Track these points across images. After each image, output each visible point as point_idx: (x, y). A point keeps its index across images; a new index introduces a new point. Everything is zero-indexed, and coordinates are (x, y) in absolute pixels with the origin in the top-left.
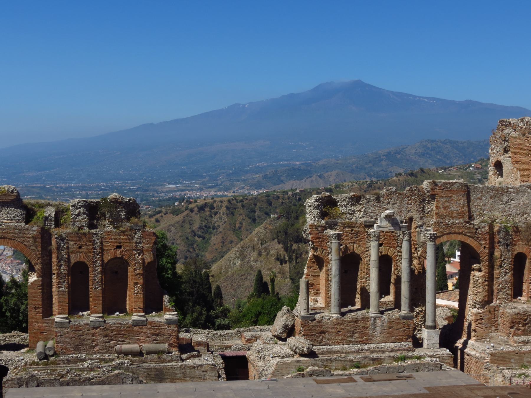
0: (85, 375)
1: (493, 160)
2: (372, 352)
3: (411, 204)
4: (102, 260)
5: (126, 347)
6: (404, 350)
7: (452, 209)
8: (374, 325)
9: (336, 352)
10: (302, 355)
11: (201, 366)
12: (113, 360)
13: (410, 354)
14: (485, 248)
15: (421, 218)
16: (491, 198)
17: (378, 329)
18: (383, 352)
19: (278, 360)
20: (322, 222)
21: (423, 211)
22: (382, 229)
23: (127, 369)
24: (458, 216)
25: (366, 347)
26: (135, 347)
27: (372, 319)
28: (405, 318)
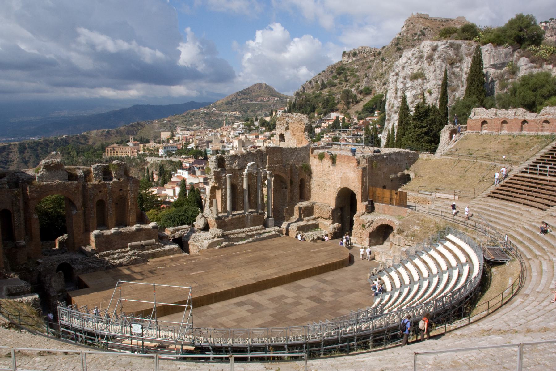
2: (248, 232)
5: (133, 243)
7: (275, 159)
10: (218, 237)
13: (265, 231)
15: (262, 165)
18: (253, 231)
20: (219, 170)
23: (138, 255)
24: (277, 163)
25: (244, 230)
26: (138, 243)
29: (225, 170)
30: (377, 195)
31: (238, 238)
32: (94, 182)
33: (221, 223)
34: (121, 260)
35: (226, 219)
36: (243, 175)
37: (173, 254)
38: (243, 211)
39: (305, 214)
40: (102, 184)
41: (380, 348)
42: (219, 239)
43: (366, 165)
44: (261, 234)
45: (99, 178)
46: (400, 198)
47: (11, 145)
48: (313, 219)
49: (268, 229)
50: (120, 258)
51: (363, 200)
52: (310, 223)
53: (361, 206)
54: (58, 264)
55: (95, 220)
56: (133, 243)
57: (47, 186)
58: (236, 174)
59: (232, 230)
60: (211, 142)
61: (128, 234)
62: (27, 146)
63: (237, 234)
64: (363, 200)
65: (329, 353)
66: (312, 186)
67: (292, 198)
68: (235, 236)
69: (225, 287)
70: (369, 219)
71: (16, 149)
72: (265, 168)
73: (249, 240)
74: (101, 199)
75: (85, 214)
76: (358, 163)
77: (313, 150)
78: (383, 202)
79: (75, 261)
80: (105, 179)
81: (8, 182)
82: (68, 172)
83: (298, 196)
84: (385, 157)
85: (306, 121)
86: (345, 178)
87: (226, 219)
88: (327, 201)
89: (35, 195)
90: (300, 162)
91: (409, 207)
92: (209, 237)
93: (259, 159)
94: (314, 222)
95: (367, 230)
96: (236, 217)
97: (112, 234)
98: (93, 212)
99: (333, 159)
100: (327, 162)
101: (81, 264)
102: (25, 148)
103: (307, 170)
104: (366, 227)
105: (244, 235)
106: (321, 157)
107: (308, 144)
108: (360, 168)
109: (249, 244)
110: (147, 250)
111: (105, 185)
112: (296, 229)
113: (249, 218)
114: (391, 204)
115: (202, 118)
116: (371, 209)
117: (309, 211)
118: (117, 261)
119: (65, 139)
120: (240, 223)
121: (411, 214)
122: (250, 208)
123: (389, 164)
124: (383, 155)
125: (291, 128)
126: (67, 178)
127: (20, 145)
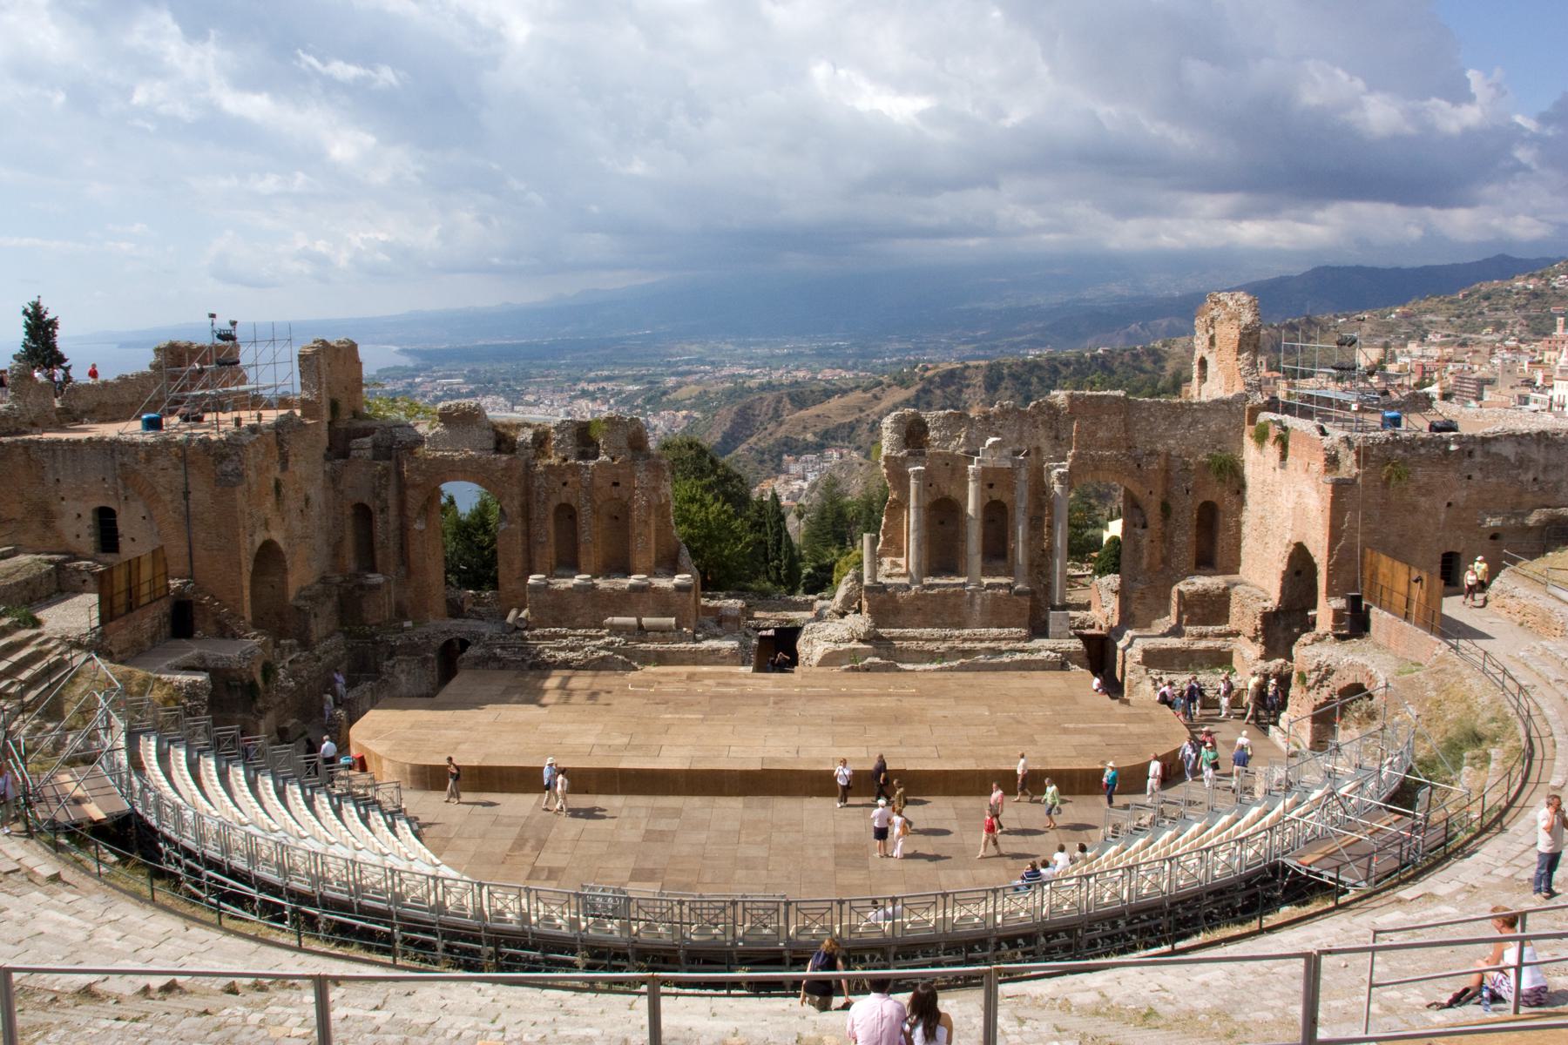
1: (1197, 356)
2: (965, 640)
5: (618, 620)
7: (1100, 434)
8: (971, 603)
10: (859, 640)
11: (719, 650)
12: (602, 637)
15: (1053, 447)
18: (982, 641)
19: (827, 645)
21: (1057, 438)
23: (618, 651)
24: (1109, 446)
25: (957, 633)
26: (633, 620)
28: (1019, 593)
29: (923, 454)
30: (1381, 580)
31: (922, 652)
32: (554, 461)
33: (884, 605)
34: (571, 655)
35: (899, 594)
36: (965, 476)
37: (716, 663)
38: (961, 580)
39: (1193, 614)
40: (569, 466)
41: (337, 952)
42: (861, 646)
43: (1355, 470)
44: (1001, 652)
45: (563, 450)
46: (1427, 600)
47: (968, 367)
48: (1219, 635)
49: (1037, 643)
50: (572, 649)
51: (1331, 593)
52: (1202, 645)
53: (1325, 610)
55: (553, 550)
56: (618, 620)
57: (443, 459)
58: (955, 467)
59: (919, 627)
60: (1489, 382)
61: (609, 595)
62: (1005, 371)
63: (927, 640)
64: (1331, 593)
65: (469, 962)
66: (1245, 530)
67: (1165, 561)
68: (913, 645)
69: (672, 759)
70: (1323, 659)
71: (979, 380)
72: (1064, 459)
73: (955, 664)
75: (527, 534)
76: (1332, 461)
77: (1254, 412)
78: (1389, 611)
79: (478, 637)
80: (583, 455)
81: (375, 446)
82: (497, 433)
83: (1187, 556)
84: (1453, 448)
85: (1247, 317)
86: (1300, 512)
87: (899, 594)
88: (1265, 584)
89: (419, 479)
90: (1203, 446)
91: (1451, 630)
92: (837, 635)
93: (1042, 431)
94: (1219, 643)
95: (1313, 693)
96: (935, 591)
97: (568, 589)
98: (548, 530)
99: (1283, 442)
100: (1272, 450)
101: (486, 646)
102: (1001, 378)
103: (1232, 475)
104: (1310, 683)
105: (944, 646)
106: (1261, 437)
107: (1239, 388)
108: (1328, 478)
109: (948, 674)
110: (652, 641)
111: (575, 469)
112: (1139, 658)
114: (1407, 617)
115: (1516, 307)
116: (1355, 624)
117: (1212, 609)
118: (561, 655)
119: (1103, 357)
120: (948, 611)
121: (1442, 660)
122: (985, 573)
123: (1477, 475)
124: (1447, 443)
125: (1217, 341)
126: (491, 444)
127: (991, 367)
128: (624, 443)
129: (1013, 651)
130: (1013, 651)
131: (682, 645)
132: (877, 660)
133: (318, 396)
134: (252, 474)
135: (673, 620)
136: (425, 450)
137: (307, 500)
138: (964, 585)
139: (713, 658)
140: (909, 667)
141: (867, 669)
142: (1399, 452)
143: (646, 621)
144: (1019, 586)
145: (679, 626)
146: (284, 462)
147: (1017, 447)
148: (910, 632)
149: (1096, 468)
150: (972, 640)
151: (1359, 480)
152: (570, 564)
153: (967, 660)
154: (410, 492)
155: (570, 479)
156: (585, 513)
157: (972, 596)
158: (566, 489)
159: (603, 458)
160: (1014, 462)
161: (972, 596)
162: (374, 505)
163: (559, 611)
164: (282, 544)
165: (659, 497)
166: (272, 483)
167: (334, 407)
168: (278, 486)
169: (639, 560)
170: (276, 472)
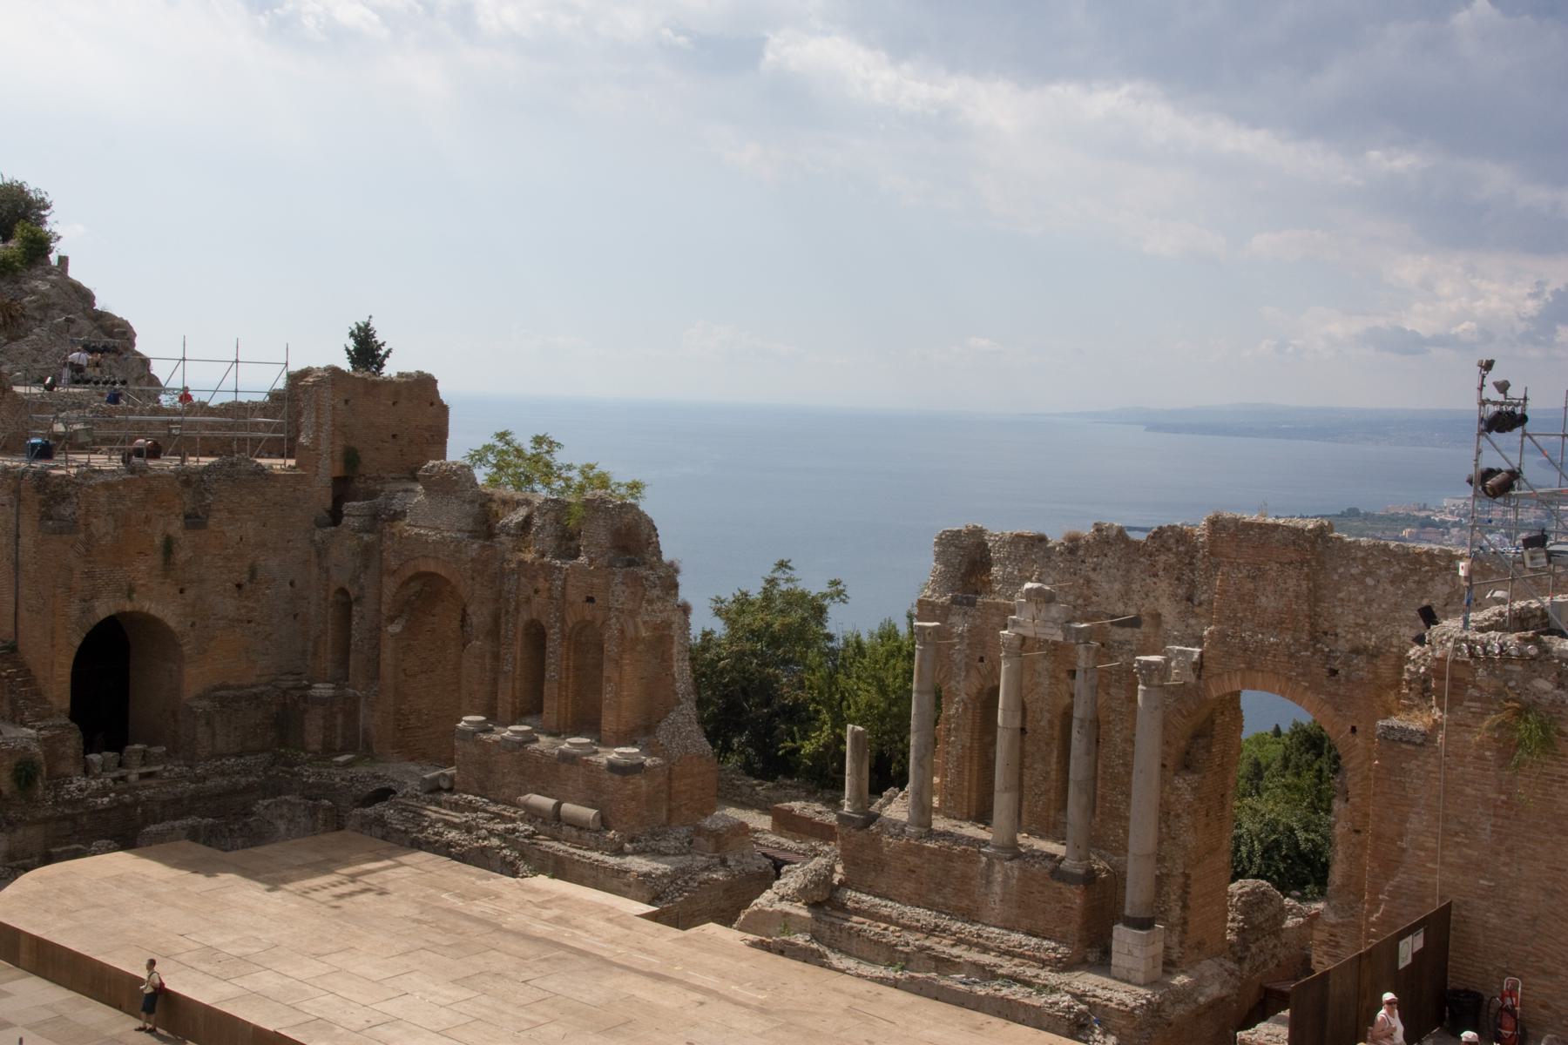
0: (453, 835)
2: (959, 942)
3: (1156, 575)
4: (563, 621)
6: (1033, 958)
9: (888, 919)
11: (626, 872)
12: (513, 820)
13: (1029, 972)
14: (1354, 729)
15: (1183, 616)
16: (1392, 582)
17: (997, 889)
18: (985, 950)
21: (1189, 599)
22: (1021, 631)
26: (548, 802)
27: (984, 859)
29: (972, 604)
31: (892, 947)
32: (529, 557)
50: (469, 830)
54: (377, 786)
63: (905, 927)
74: (535, 616)
75: (496, 657)
87: (885, 838)
89: (394, 564)
93: (1163, 586)
98: (516, 652)
111: (549, 570)
113: (999, 877)
128: (604, 538)
129: (1013, 979)
130: (1013, 979)
131: (596, 855)
132: (801, 939)
133: (316, 439)
134: (102, 526)
135: (590, 813)
136: (405, 527)
137: (253, 573)
138: (985, 843)
139: (615, 882)
140: (850, 963)
141: (783, 950)
142: (1543, 685)
143: (569, 808)
144: (1065, 865)
145: (605, 823)
146: (194, 521)
147: (1119, 608)
148: (889, 908)
149: (1250, 667)
150: (971, 945)
151: (1440, 737)
152: (531, 708)
153: (925, 975)
154: (385, 579)
155: (541, 584)
156: (554, 635)
157: (990, 865)
158: (537, 599)
159: (583, 559)
160: (1067, 631)
161: (990, 865)
162: (353, 591)
163: (493, 777)
164: (172, 622)
165: (636, 627)
166: (158, 541)
167: (351, 458)
168: (169, 546)
169: (609, 722)
170: (176, 527)
